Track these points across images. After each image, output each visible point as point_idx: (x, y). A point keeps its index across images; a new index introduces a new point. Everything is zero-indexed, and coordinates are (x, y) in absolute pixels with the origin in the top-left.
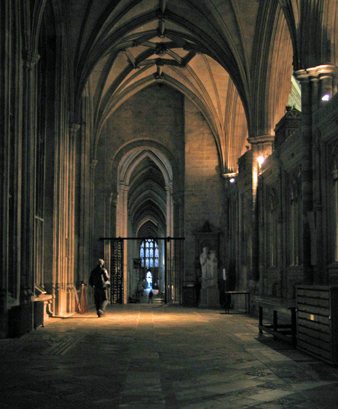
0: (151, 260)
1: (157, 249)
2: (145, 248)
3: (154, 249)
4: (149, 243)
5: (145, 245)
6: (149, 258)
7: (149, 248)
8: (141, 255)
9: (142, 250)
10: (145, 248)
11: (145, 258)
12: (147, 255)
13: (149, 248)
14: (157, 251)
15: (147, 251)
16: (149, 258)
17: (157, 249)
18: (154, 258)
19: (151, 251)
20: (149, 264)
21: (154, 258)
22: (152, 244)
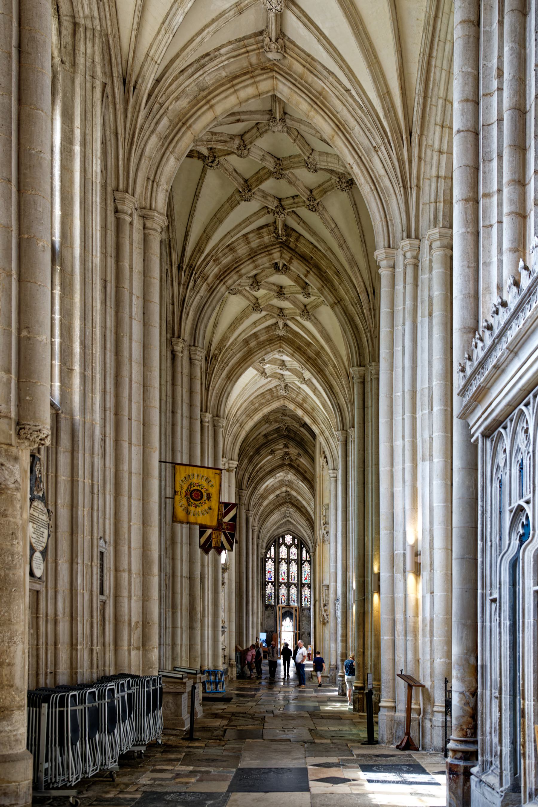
0: (293, 591)
1: (306, 564)
2: (277, 561)
3: (300, 563)
4: (289, 547)
5: (277, 553)
6: (288, 585)
7: (288, 562)
8: (267, 575)
9: (270, 565)
10: (277, 561)
11: (277, 584)
12: (283, 577)
13: (288, 562)
14: (306, 568)
15: (283, 567)
16: (288, 585)
17: (306, 564)
18: (300, 586)
19: (293, 568)
20: (288, 599)
21: (300, 586)
22: (293, 550)
